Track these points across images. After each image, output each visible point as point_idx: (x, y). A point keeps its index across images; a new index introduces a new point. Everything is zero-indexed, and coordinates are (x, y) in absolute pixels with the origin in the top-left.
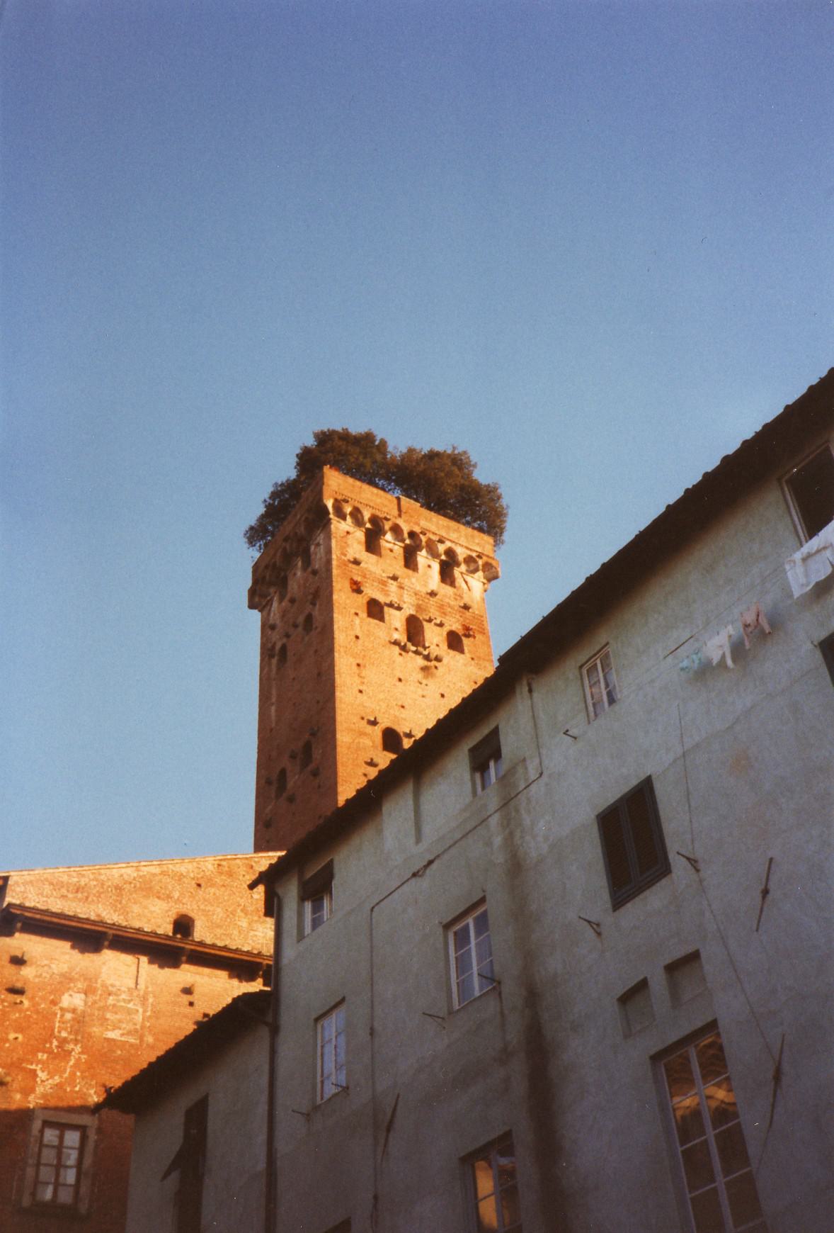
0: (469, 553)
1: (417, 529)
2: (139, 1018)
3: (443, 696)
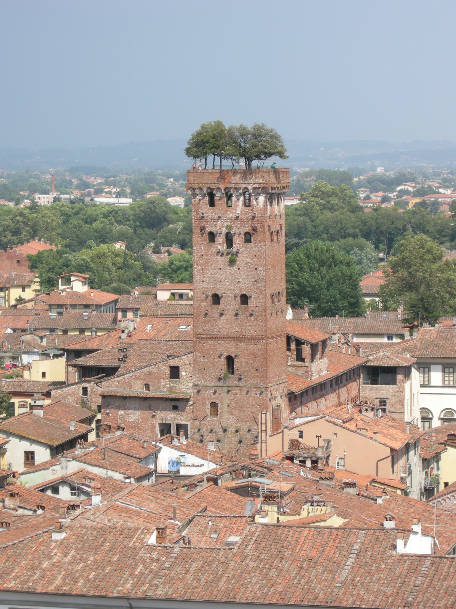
0: (254, 186)
1: (229, 186)
2: (137, 415)
3: (239, 269)
